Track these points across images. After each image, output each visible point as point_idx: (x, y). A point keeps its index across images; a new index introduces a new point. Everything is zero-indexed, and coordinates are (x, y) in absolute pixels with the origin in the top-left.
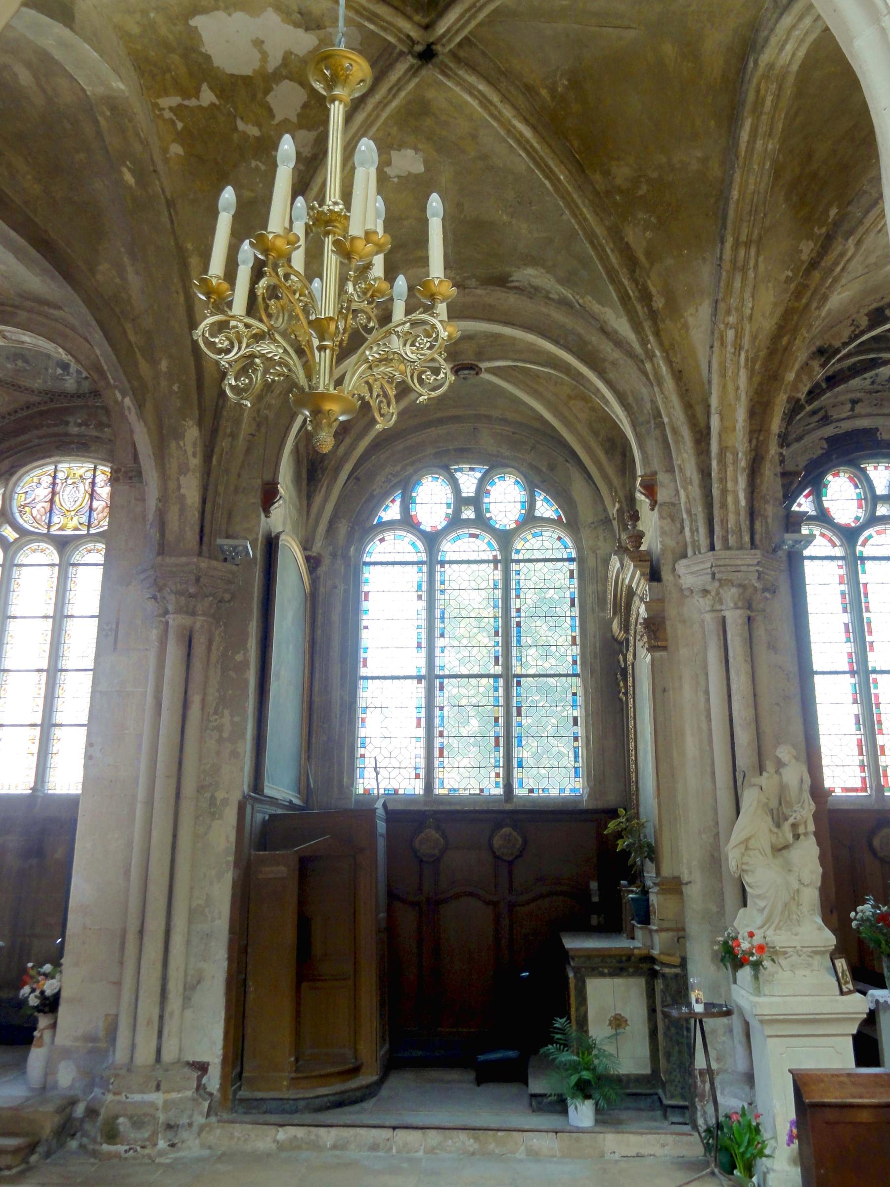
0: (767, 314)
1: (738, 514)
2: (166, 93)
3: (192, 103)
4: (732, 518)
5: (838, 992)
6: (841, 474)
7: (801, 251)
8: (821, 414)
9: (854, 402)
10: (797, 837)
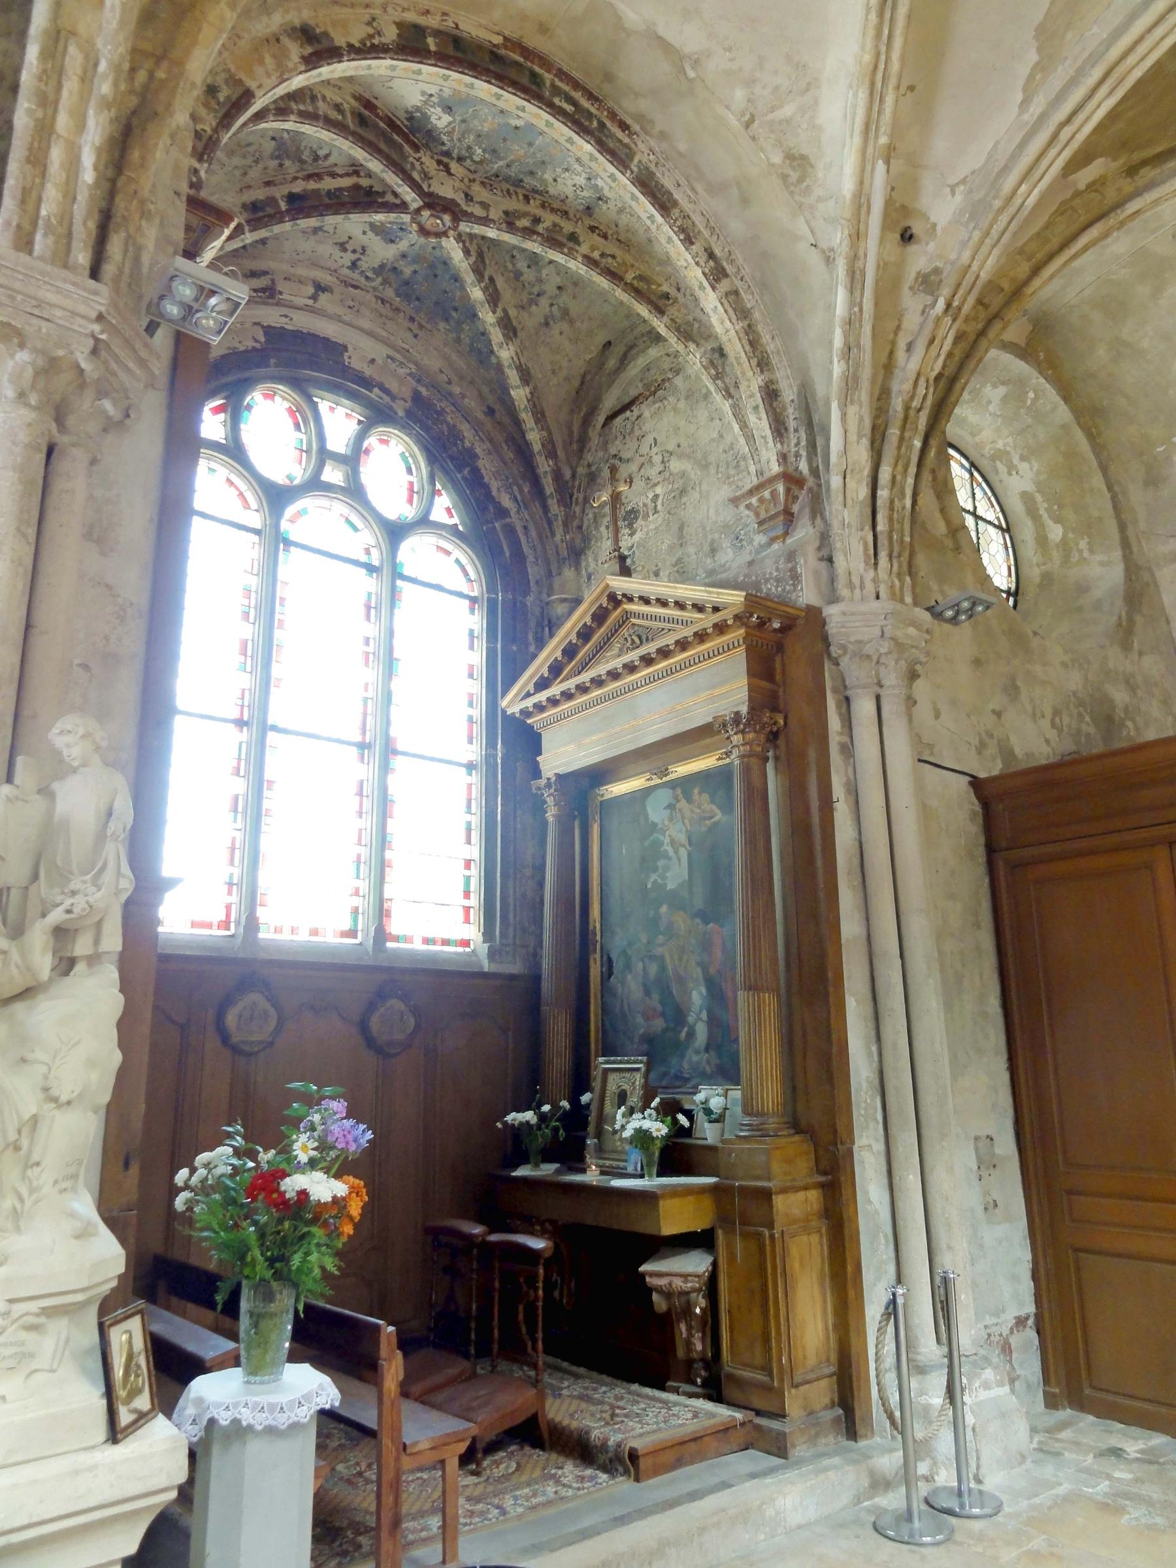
1: (70, 196)
4: (52, 195)
5: (102, 1432)
9: (320, 288)
10: (66, 965)
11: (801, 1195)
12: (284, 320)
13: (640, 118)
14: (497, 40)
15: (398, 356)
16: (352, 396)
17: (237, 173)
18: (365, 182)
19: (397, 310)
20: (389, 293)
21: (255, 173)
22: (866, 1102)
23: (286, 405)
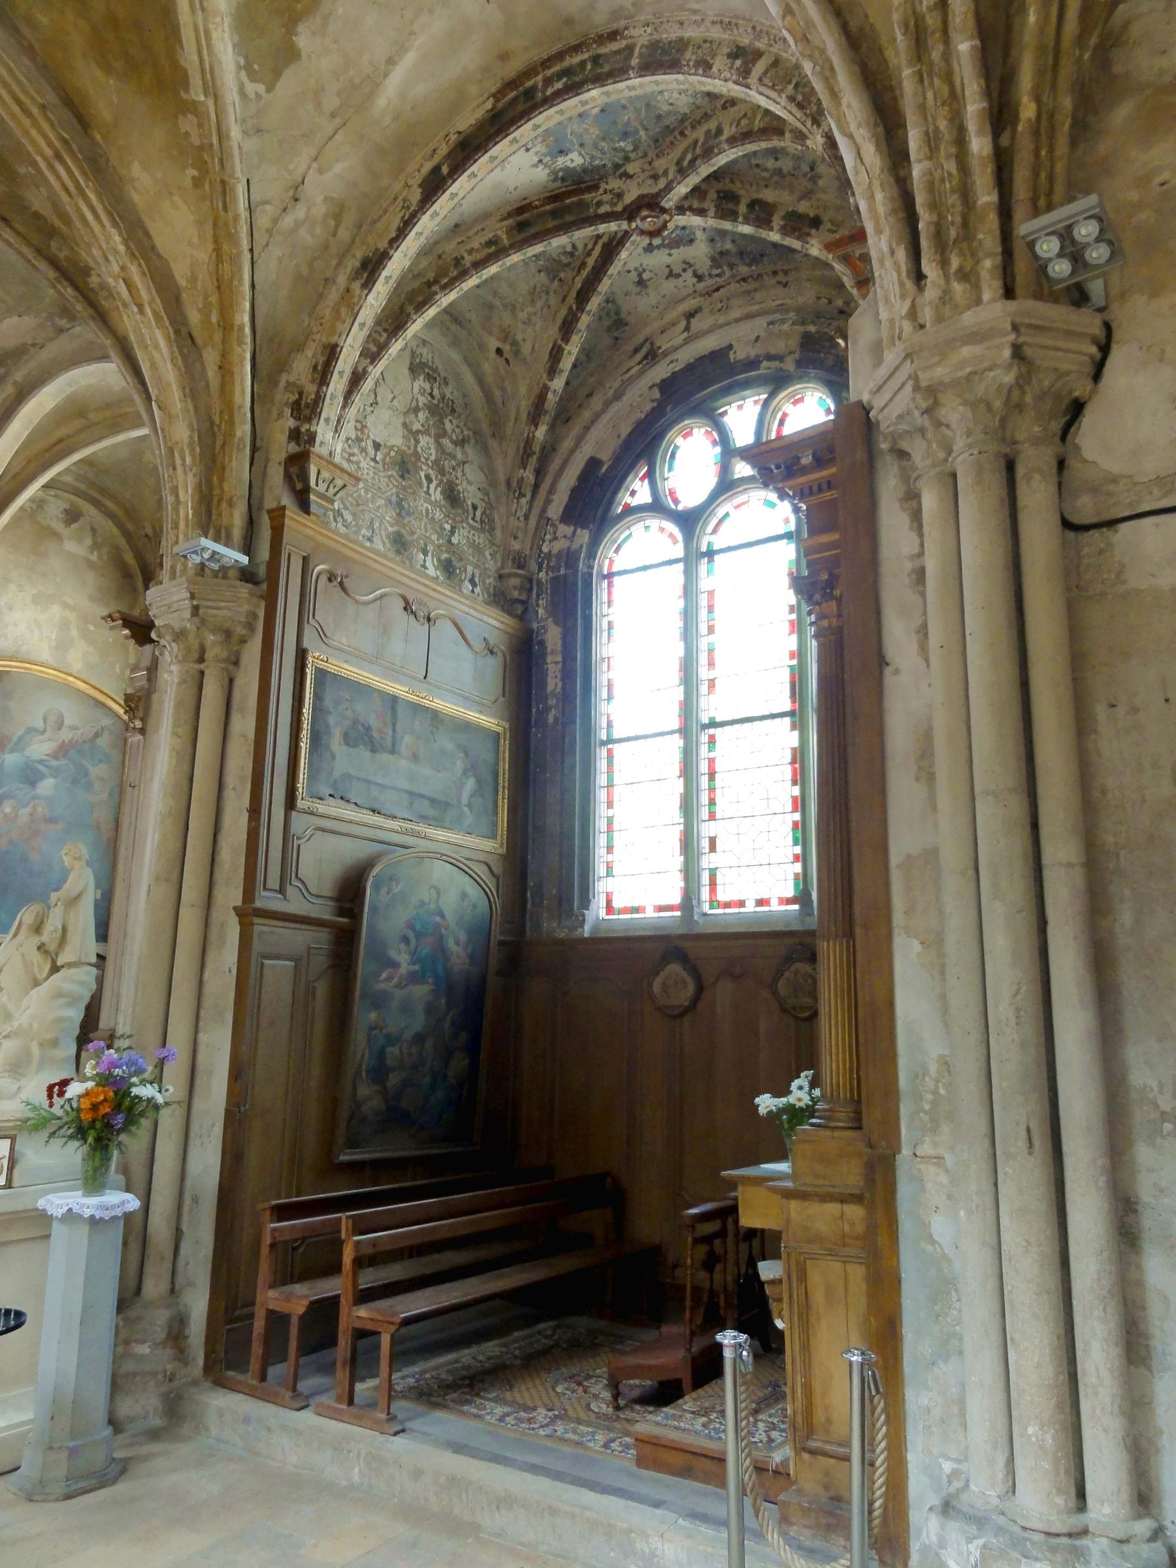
0: (195, 240)
6: (695, 431)
7: (187, 134)
8: (644, 350)
9: (690, 315)
11: (834, 1208)
12: (671, 366)
13: (615, 14)
14: (489, 105)
15: (777, 316)
16: (747, 384)
17: (545, 311)
18: (605, 239)
19: (760, 276)
20: (744, 270)
21: (553, 300)
22: (935, 1093)
23: (703, 430)
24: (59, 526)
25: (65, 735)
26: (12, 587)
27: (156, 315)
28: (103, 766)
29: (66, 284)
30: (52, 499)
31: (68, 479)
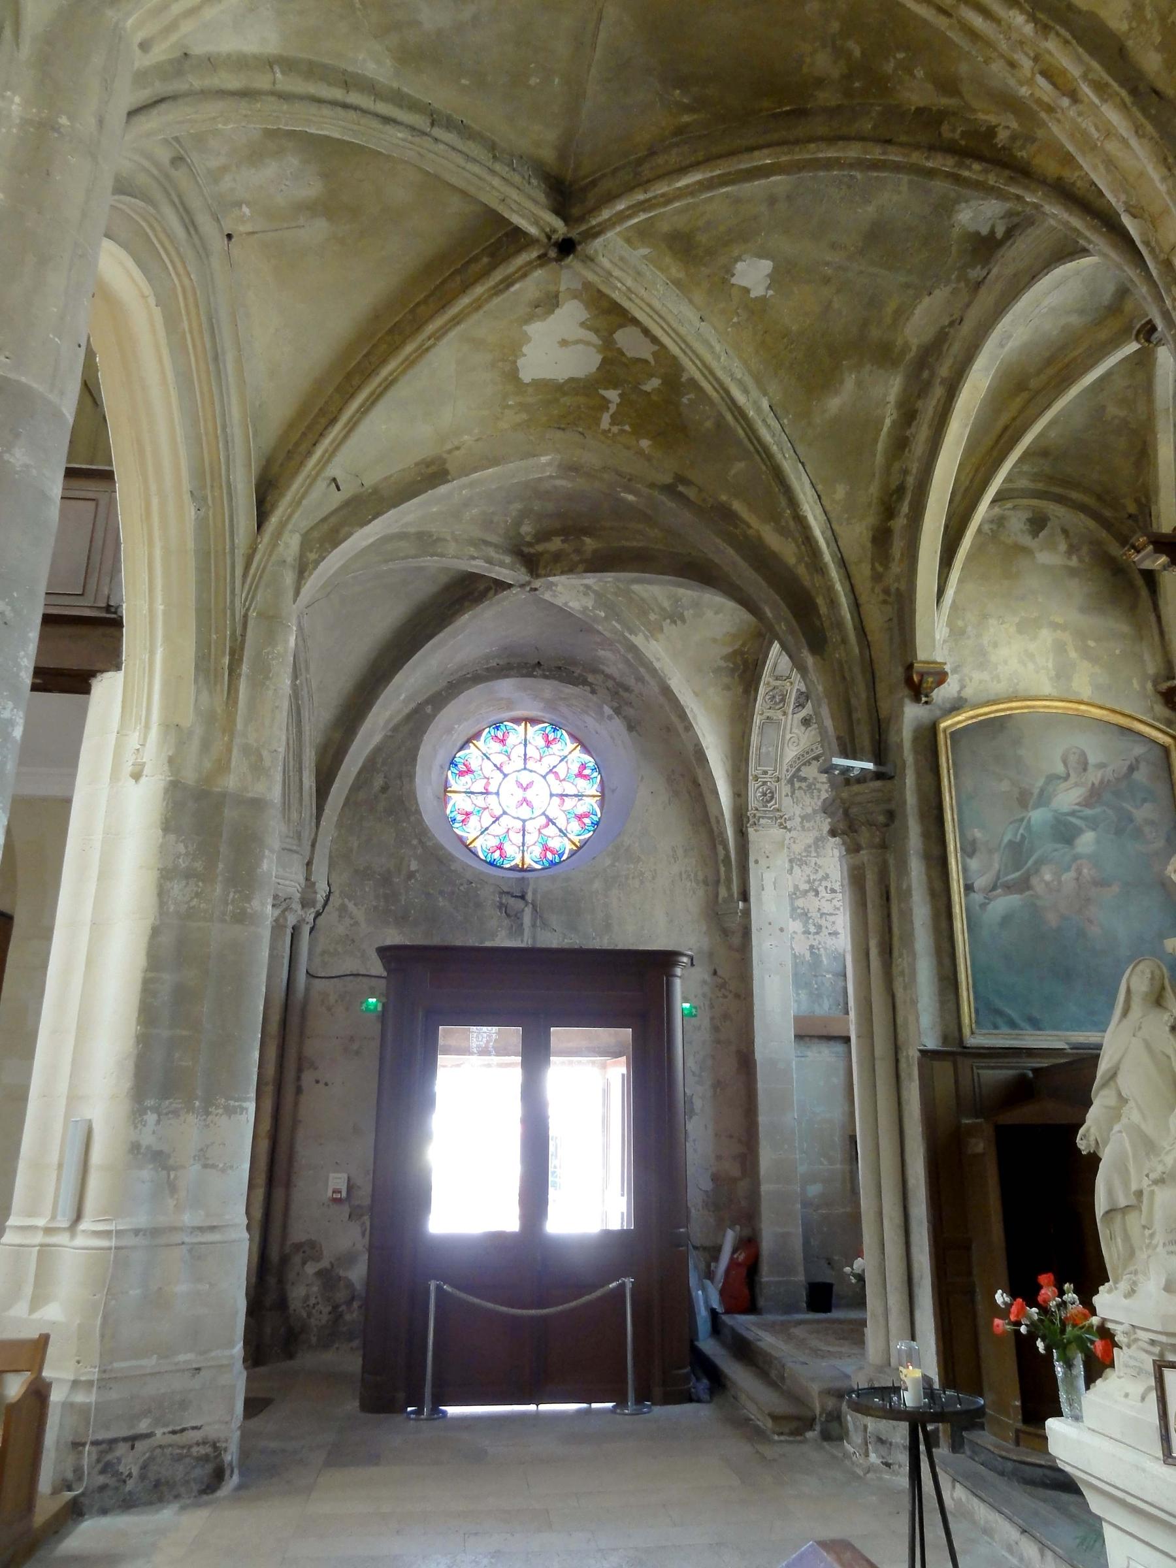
2: (597, 421)
3: (613, 408)
24: (1027, 540)
25: (1094, 776)
26: (992, 622)
27: (1100, 87)
28: (1147, 806)
29: (968, 162)
30: (1007, 513)
31: (1023, 483)
